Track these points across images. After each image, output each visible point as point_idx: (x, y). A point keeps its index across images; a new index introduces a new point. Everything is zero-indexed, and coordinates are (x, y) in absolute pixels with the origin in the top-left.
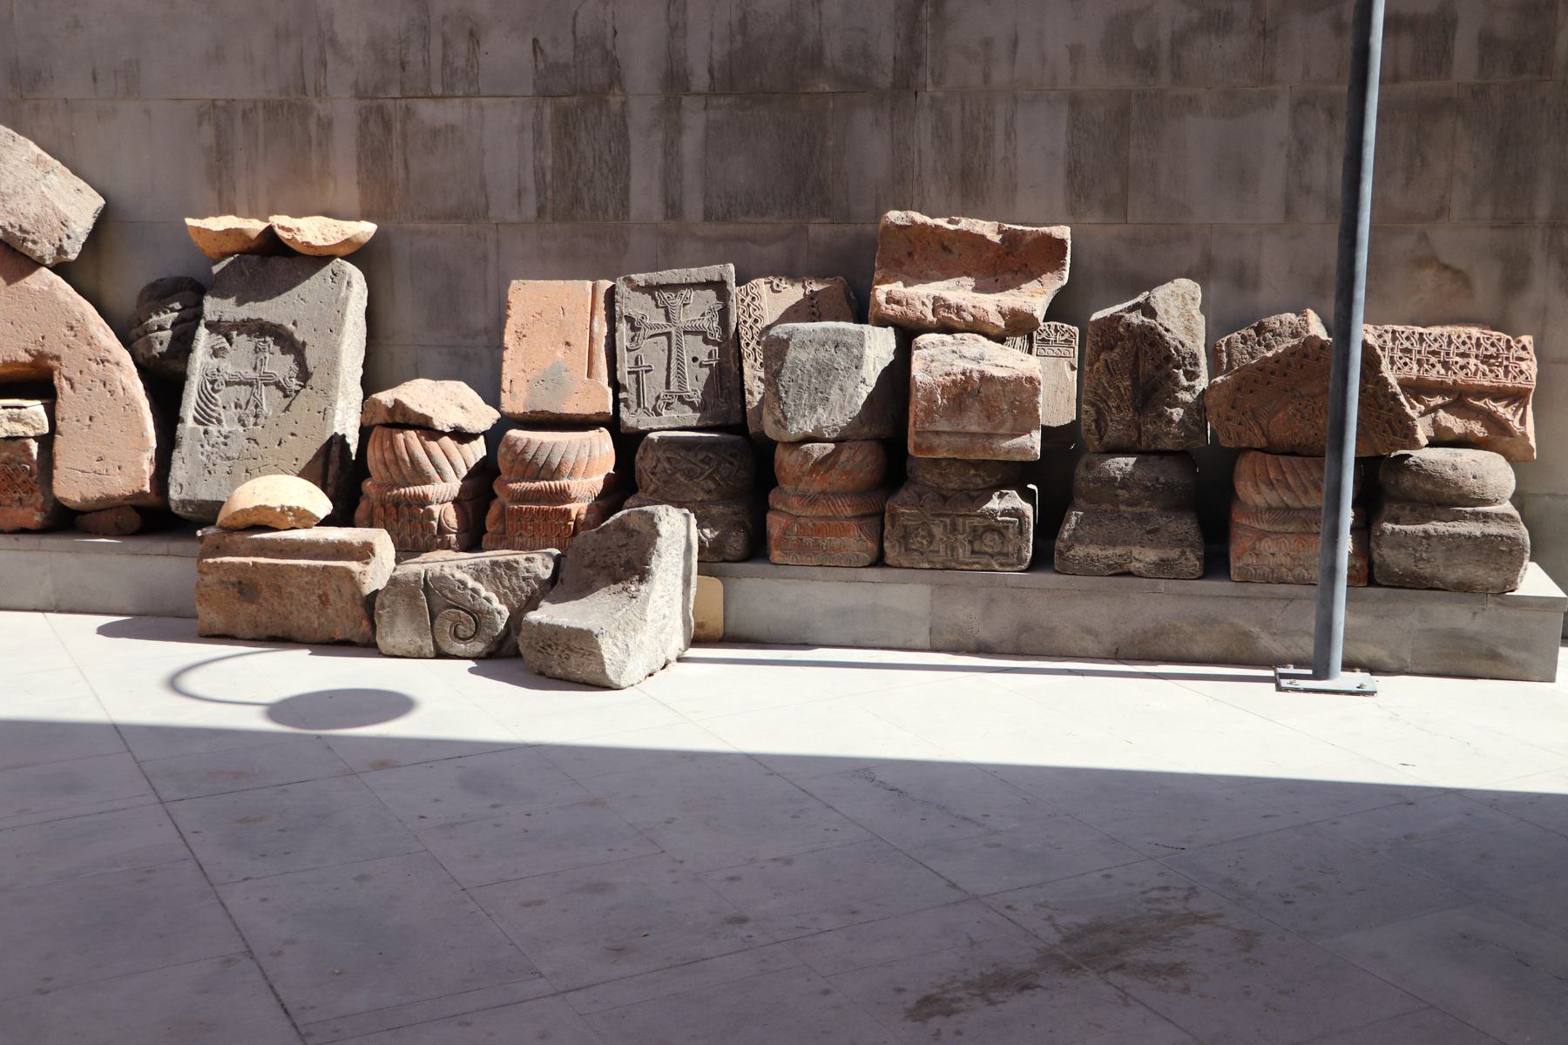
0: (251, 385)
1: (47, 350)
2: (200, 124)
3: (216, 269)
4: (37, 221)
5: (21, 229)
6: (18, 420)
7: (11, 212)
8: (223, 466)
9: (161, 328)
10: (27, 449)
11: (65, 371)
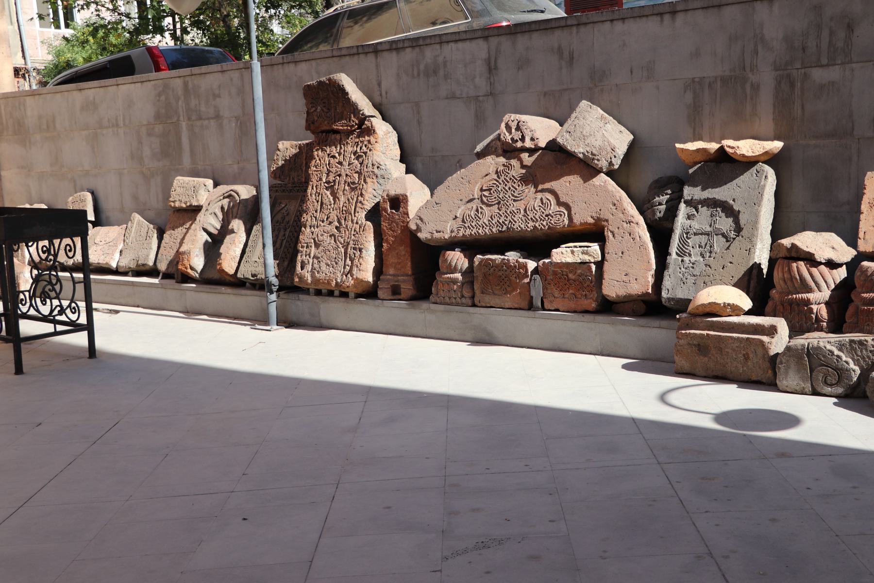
0: (708, 235)
1: (602, 216)
2: (685, 92)
3: (691, 171)
5: (592, 154)
6: (587, 253)
7: (588, 145)
8: (691, 280)
9: (660, 204)
10: (590, 268)
11: (610, 227)
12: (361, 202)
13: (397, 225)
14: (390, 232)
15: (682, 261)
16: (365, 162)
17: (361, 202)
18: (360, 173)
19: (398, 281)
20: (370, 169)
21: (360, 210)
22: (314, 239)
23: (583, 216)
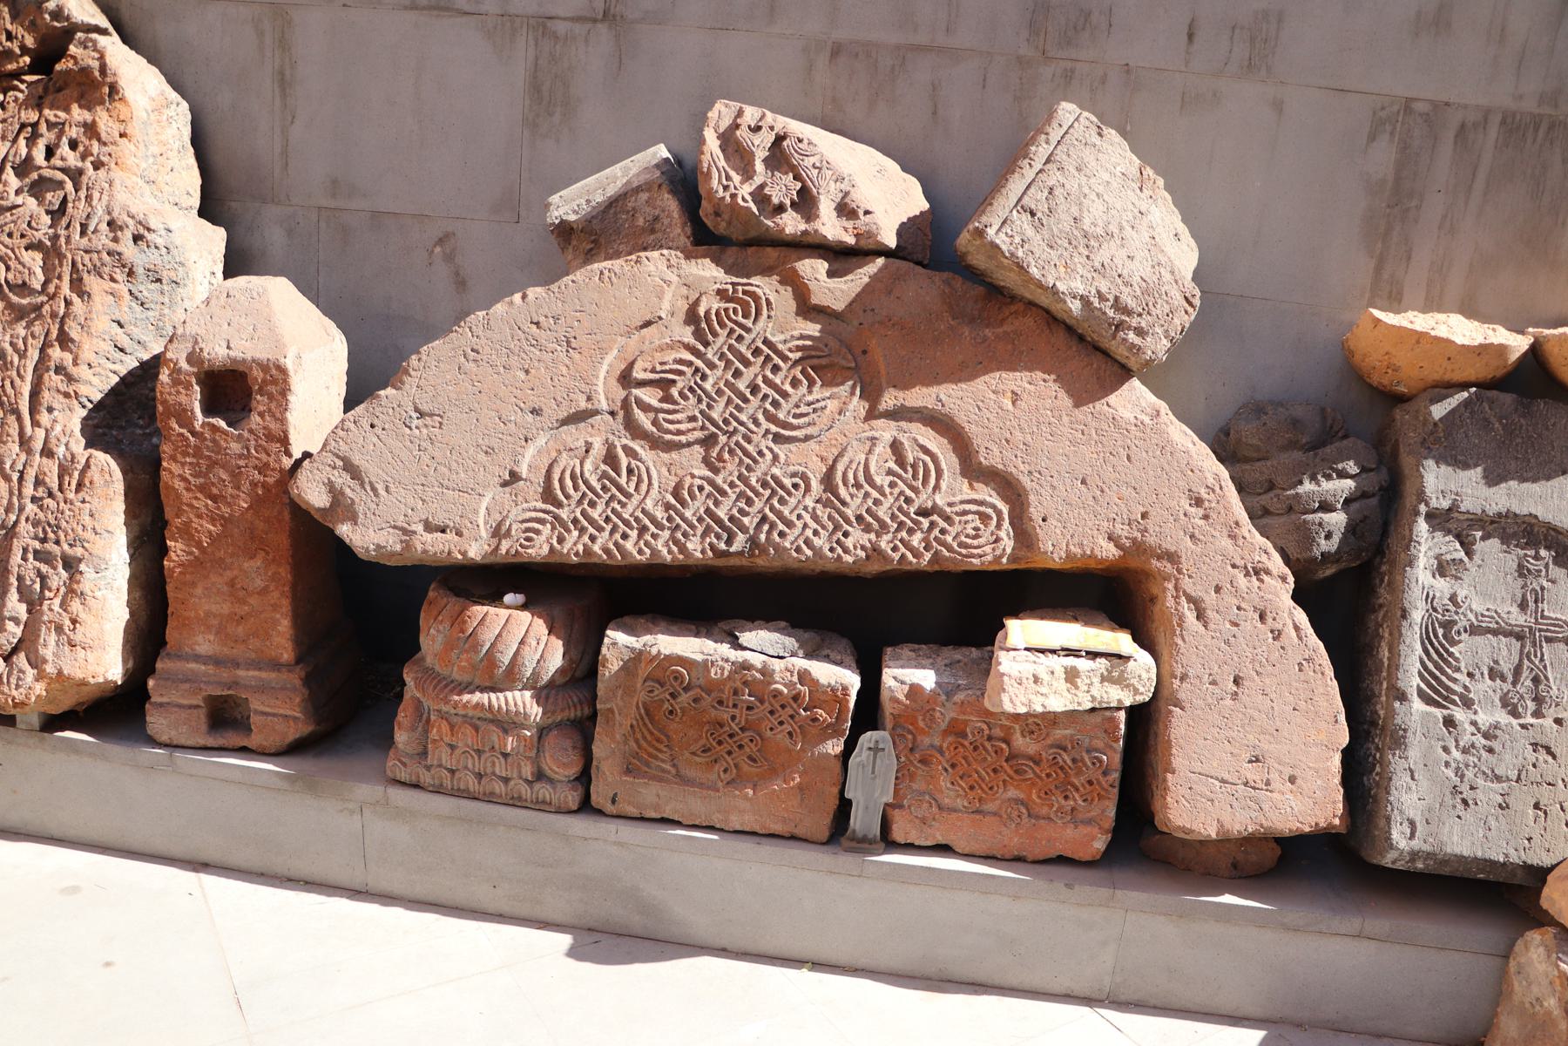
0: (1519, 637)
1: (1151, 540)
2: (1372, 138)
3: (1438, 411)
4: (1146, 292)
5: (1117, 305)
6: (1120, 681)
7: (1101, 270)
8: (1489, 793)
9: (1326, 507)
10: (1113, 720)
11: (1186, 583)
12: (59, 370)
13: (236, 475)
14: (203, 503)
15: (1449, 722)
16: (77, 211)
17: (59, 370)
18: (51, 253)
19: (235, 684)
20: (103, 239)
21: (58, 402)
23: (1072, 533)
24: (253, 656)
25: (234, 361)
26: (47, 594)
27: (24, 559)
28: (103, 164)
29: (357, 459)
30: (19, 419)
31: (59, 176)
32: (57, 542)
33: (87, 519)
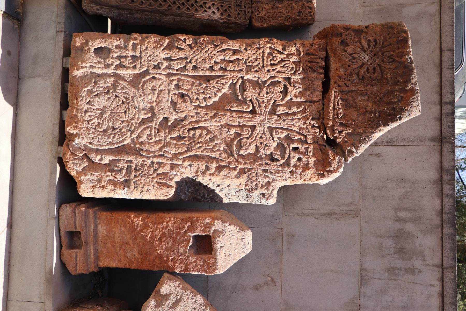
12: (207, 168)
13: (170, 249)
14: (158, 234)
16: (273, 167)
17: (207, 168)
18: (255, 157)
19: (87, 243)
20: (262, 181)
21: (194, 168)
22: (146, 73)
24: (100, 250)
25: (216, 251)
26: (113, 174)
27: (128, 161)
28: (292, 175)
29: (181, 304)
30: (186, 152)
31: (287, 156)
32: (135, 176)
33: (146, 189)
